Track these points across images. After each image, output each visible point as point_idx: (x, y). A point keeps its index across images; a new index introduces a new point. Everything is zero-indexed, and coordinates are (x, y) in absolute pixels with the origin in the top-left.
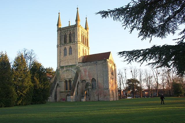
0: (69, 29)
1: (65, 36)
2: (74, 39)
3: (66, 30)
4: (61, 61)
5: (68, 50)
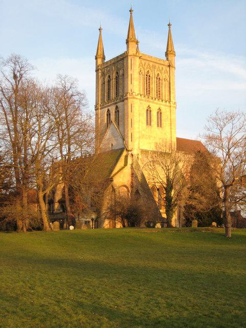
0: (157, 65)
3: (151, 64)
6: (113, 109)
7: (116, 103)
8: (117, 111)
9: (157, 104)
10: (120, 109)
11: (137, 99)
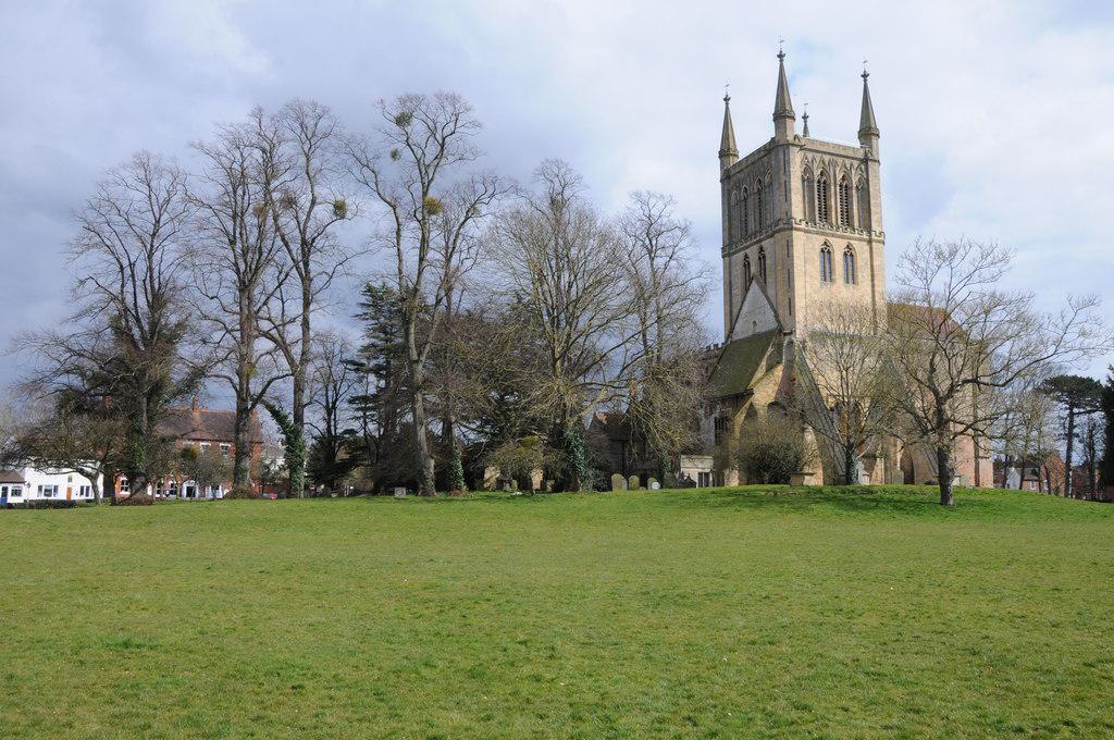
0: (840, 160)
3: (827, 158)
5: (838, 257)
6: (753, 253)
7: (760, 241)
8: (762, 258)
9: (843, 237)
10: (766, 253)
11: (799, 230)
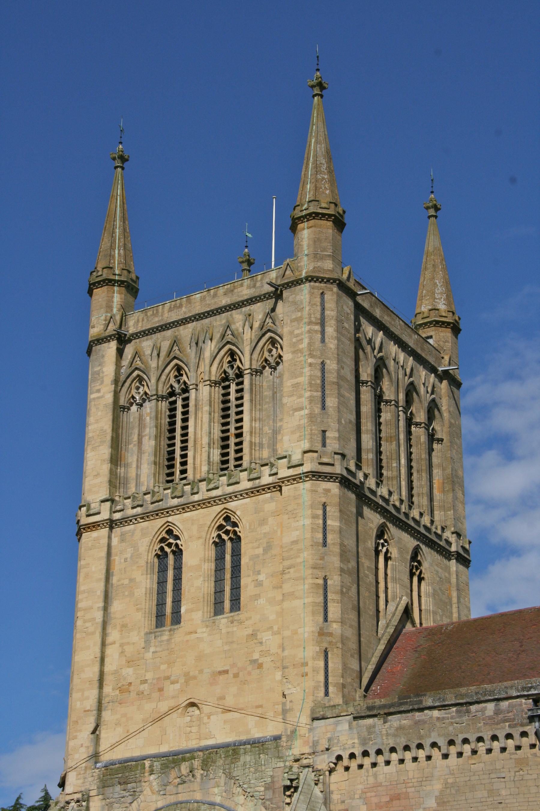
0: (219, 321)
1: (176, 397)
2: (276, 432)
3: (186, 332)
4: (107, 689)
5: (197, 557)
